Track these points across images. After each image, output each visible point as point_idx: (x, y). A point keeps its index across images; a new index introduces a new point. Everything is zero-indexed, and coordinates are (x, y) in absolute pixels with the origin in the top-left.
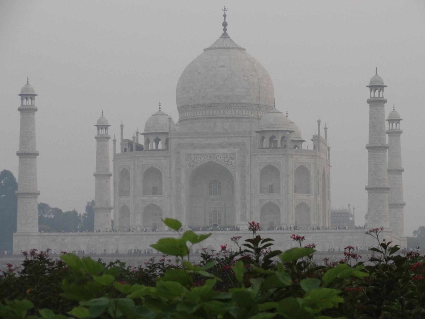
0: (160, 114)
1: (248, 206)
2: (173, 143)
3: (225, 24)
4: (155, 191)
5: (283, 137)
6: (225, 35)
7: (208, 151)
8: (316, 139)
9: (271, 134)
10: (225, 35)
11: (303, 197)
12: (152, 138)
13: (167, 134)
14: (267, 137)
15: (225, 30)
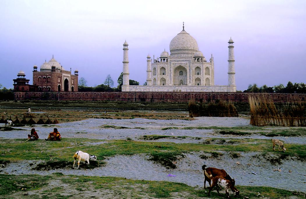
0: (165, 52)
1: (191, 79)
2: (169, 60)
3: (183, 27)
4: (163, 74)
5: (201, 59)
6: (183, 30)
7: (179, 62)
8: (211, 60)
9: (198, 58)
10: (183, 30)
11: (207, 76)
12: (163, 59)
13: (167, 57)
14: (197, 58)
15: (183, 29)
